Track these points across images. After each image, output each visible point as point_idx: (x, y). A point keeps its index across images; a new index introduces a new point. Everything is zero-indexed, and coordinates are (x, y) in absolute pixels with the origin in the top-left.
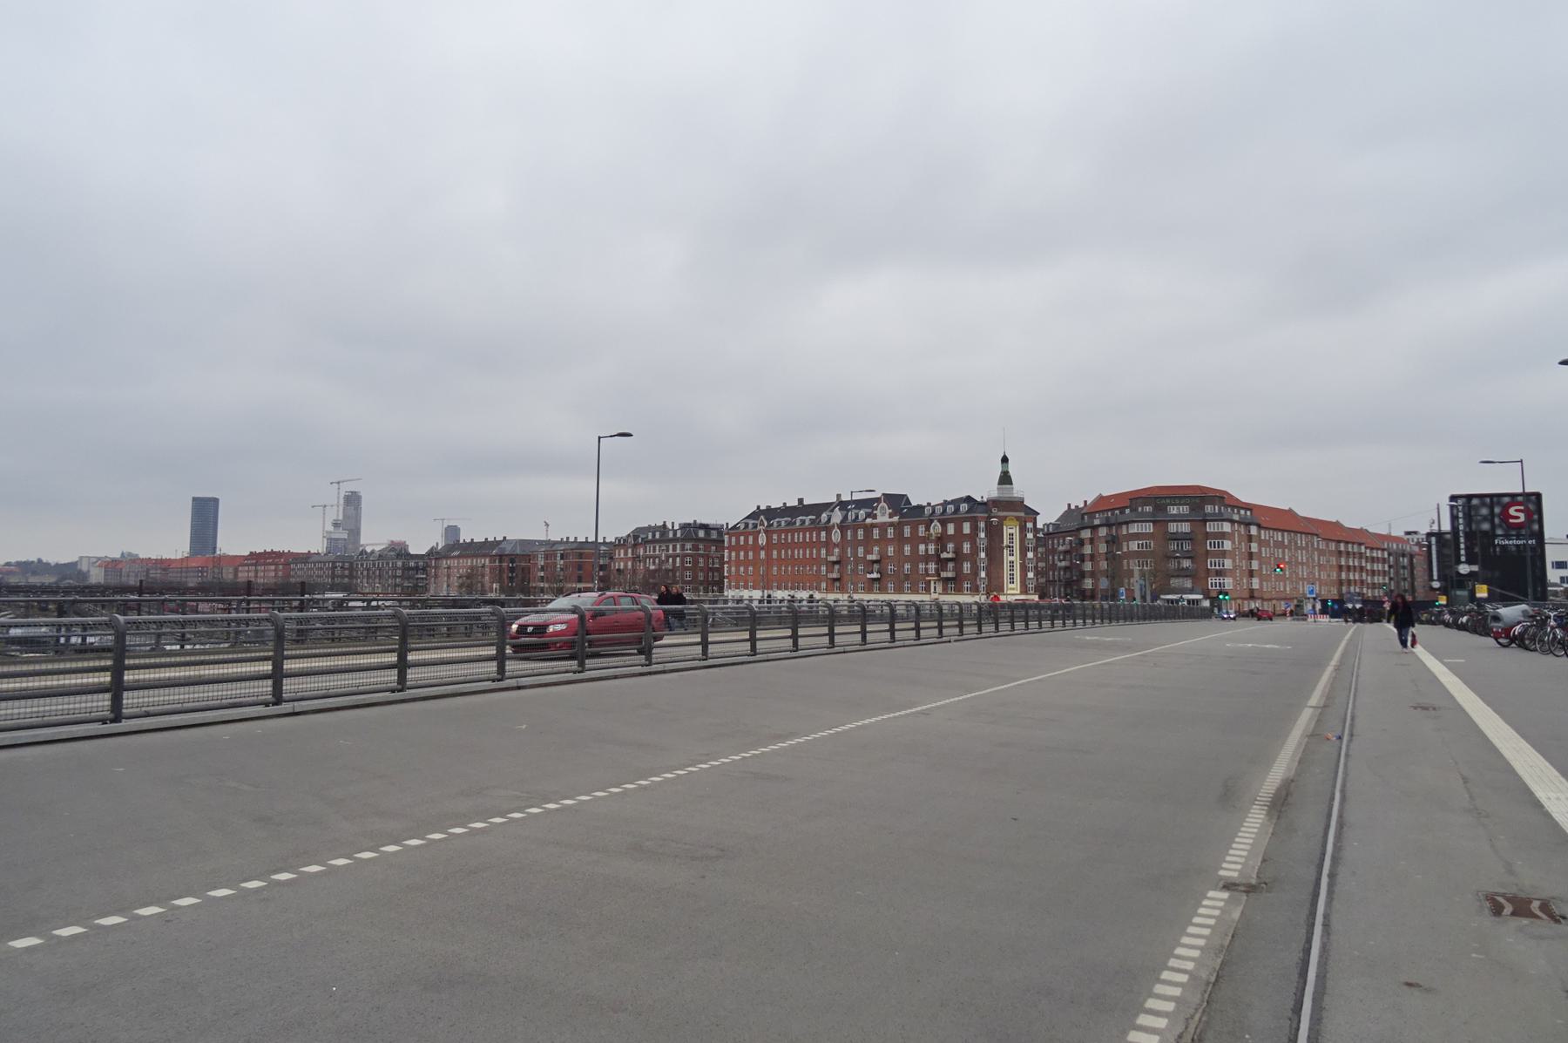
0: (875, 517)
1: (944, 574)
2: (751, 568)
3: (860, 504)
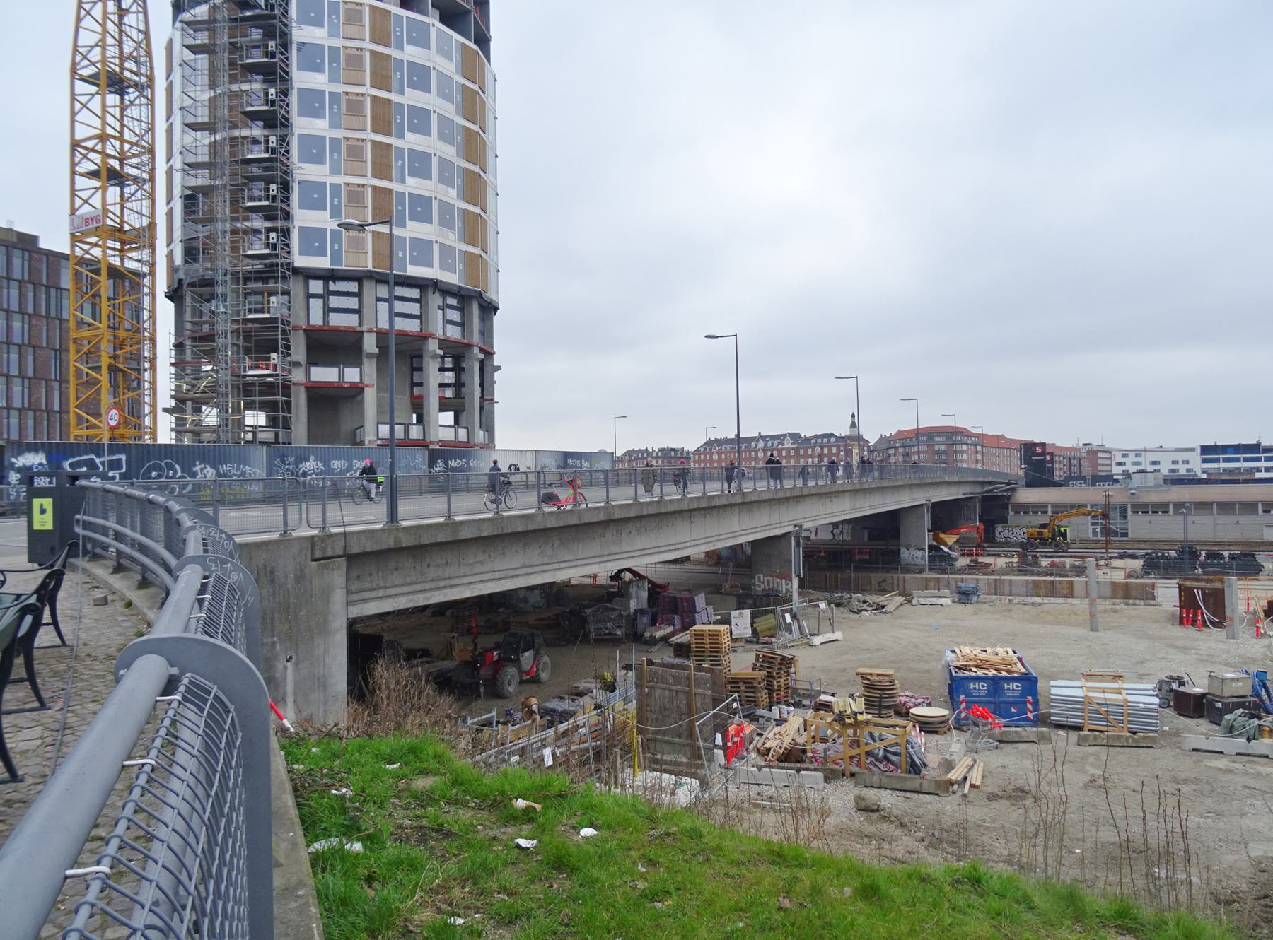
3: (773, 438)
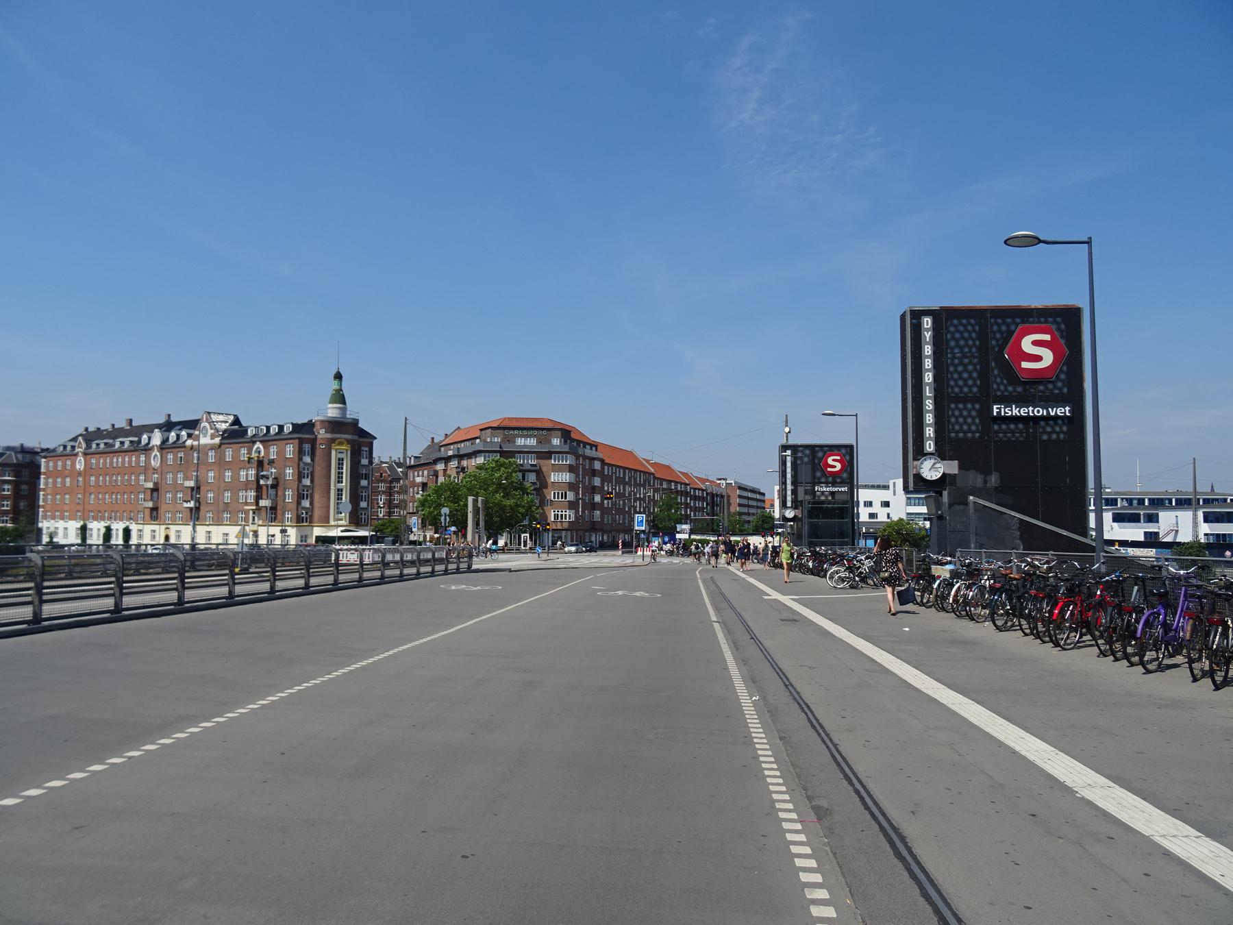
0: (197, 438)
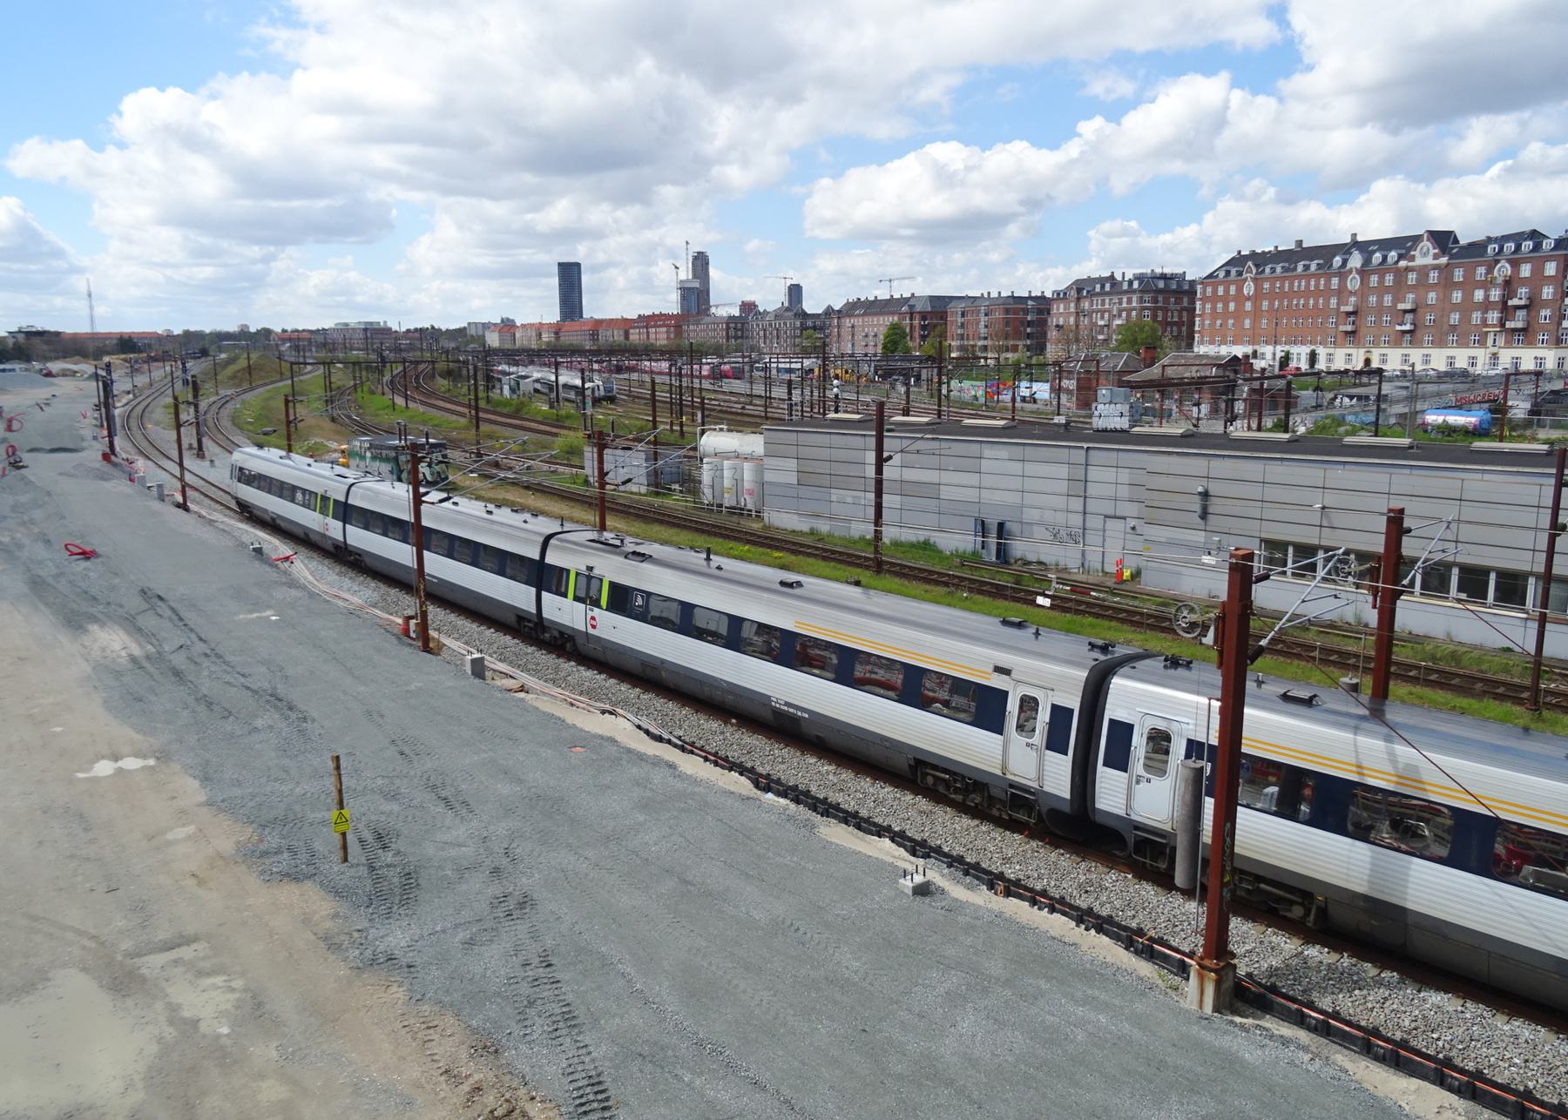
0: (1413, 258)
1: (1509, 325)
2: (1231, 322)
3: (1385, 245)
